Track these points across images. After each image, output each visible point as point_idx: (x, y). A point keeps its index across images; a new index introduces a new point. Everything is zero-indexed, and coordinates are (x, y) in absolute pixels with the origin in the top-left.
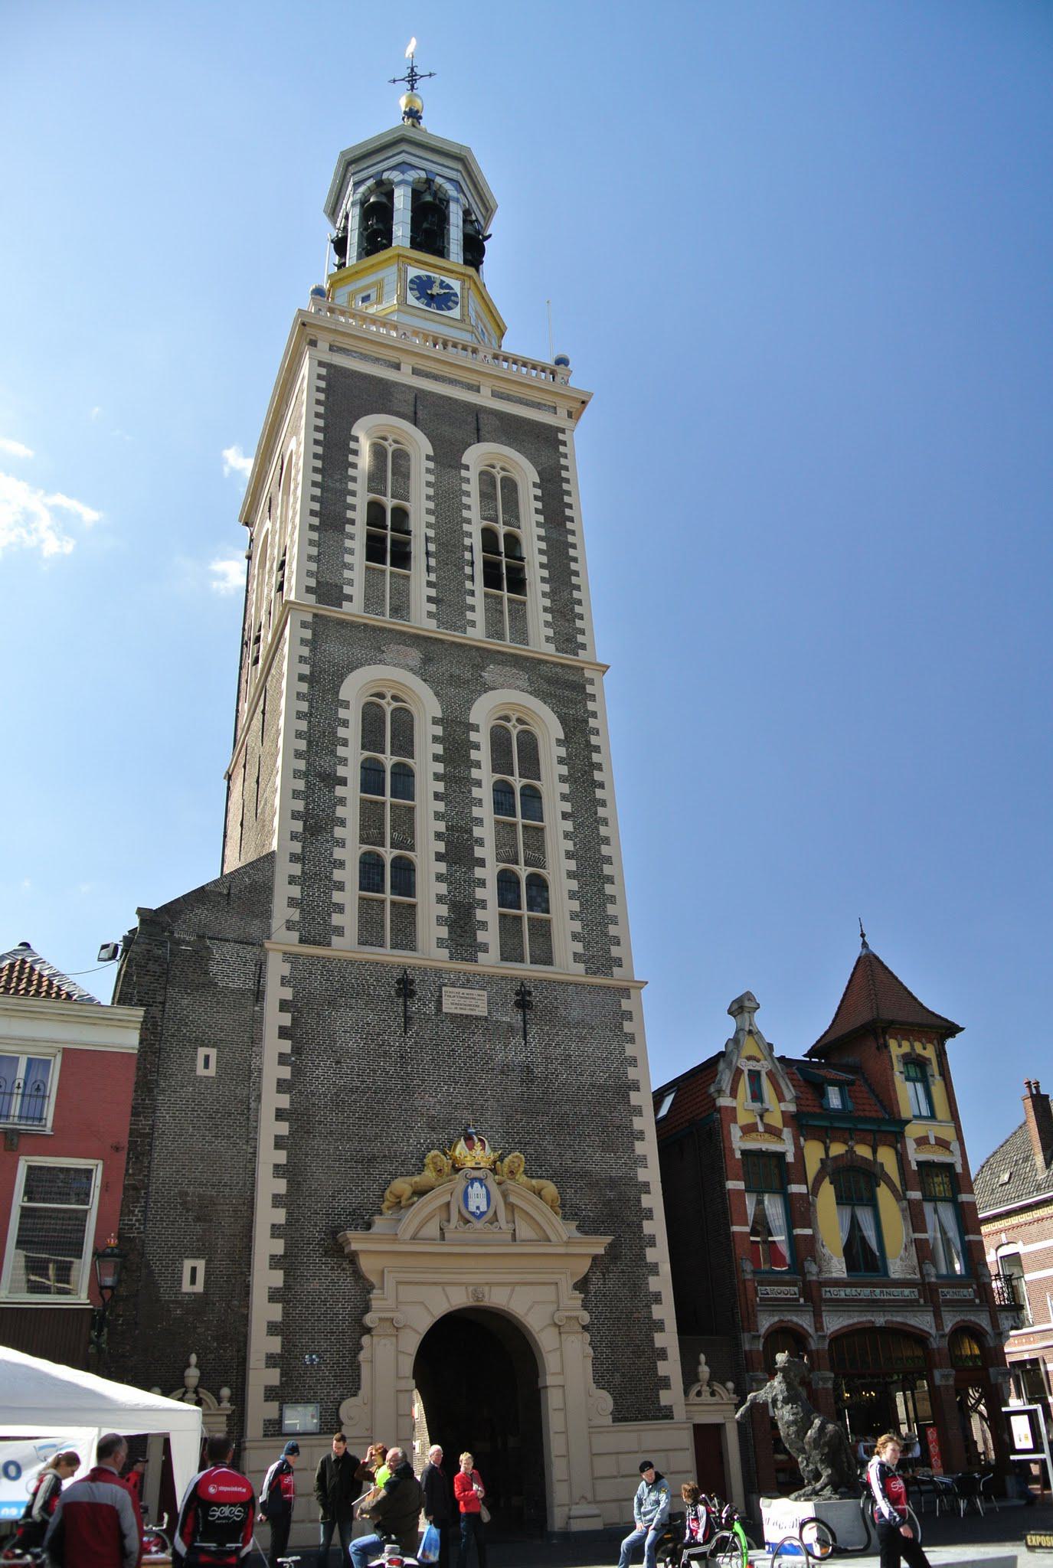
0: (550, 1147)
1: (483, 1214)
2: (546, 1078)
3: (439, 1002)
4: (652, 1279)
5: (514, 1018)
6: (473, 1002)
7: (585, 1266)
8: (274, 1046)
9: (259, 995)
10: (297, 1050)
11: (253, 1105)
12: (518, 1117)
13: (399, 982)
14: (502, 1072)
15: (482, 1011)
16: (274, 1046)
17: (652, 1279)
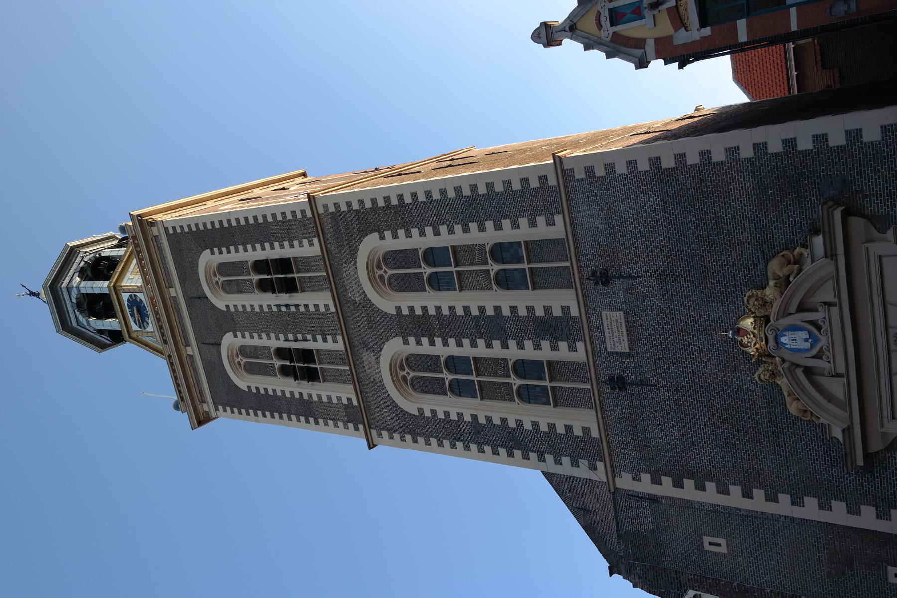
0: (734, 255)
1: (810, 333)
2: (668, 257)
3: (622, 354)
4: (867, 137)
5: (618, 286)
6: (614, 324)
7: (857, 224)
8: (689, 492)
9: (653, 499)
10: (691, 476)
11: (745, 513)
12: (710, 286)
13: (613, 388)
14: (670, 300)
15: (620, 316)
16: (689, 492)
17: (867, 137)
